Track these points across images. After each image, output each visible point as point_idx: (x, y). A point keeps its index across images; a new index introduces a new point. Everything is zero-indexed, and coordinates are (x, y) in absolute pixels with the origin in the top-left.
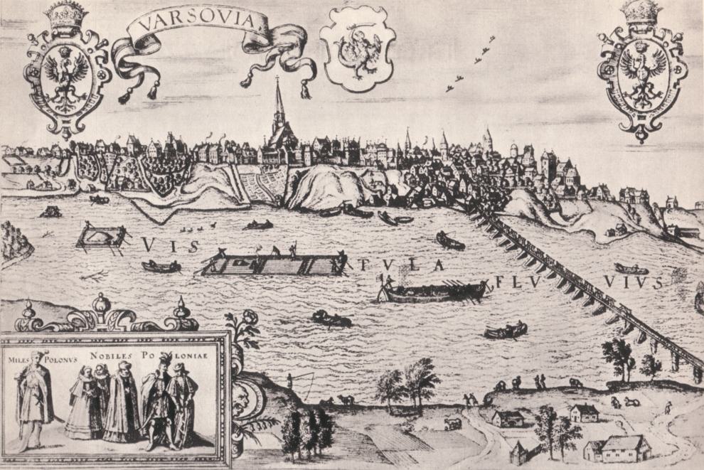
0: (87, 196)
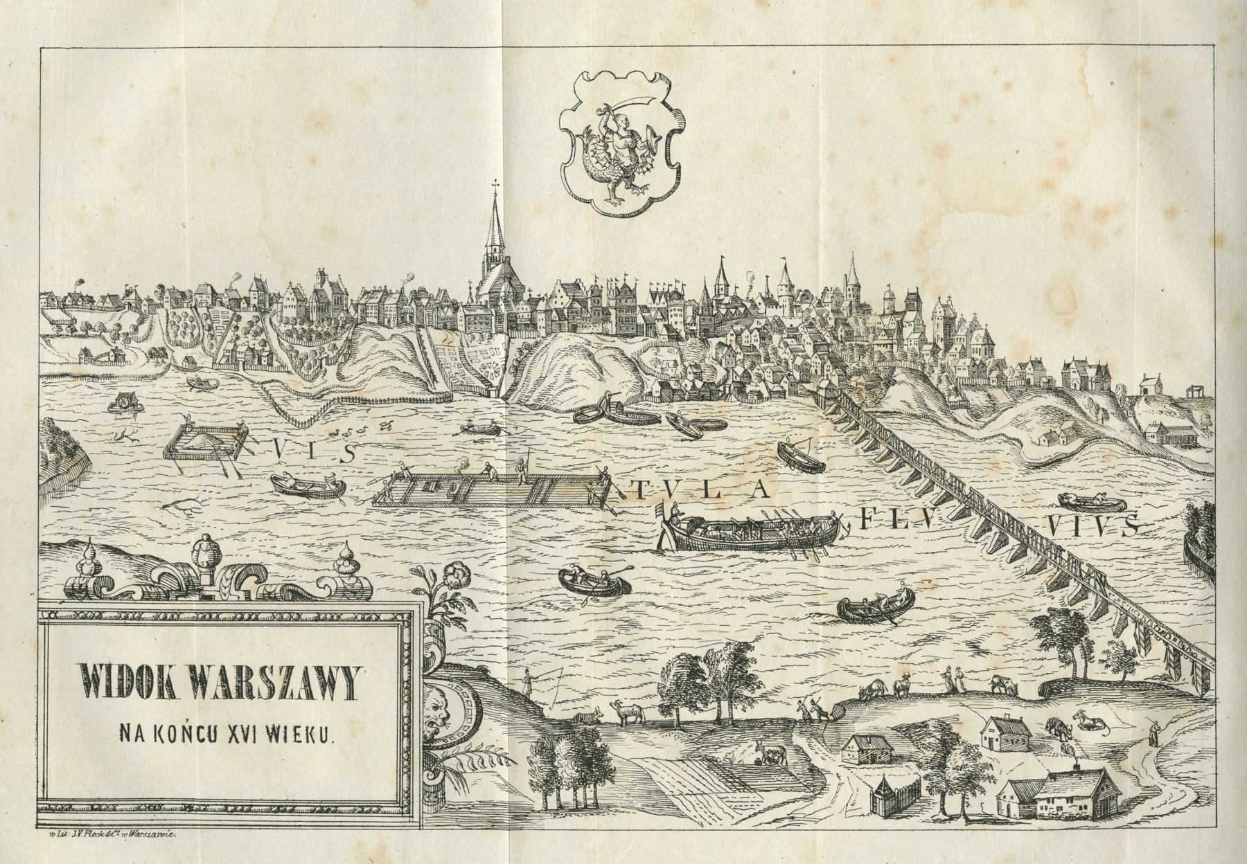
0: (183, 377)
